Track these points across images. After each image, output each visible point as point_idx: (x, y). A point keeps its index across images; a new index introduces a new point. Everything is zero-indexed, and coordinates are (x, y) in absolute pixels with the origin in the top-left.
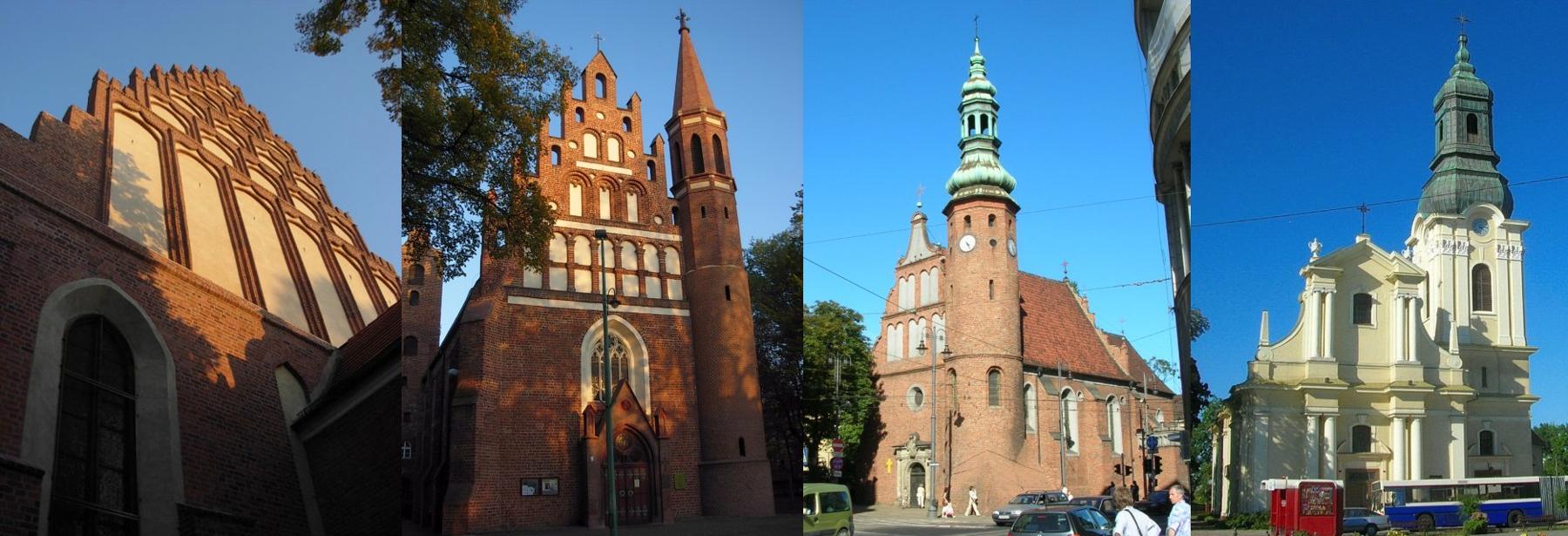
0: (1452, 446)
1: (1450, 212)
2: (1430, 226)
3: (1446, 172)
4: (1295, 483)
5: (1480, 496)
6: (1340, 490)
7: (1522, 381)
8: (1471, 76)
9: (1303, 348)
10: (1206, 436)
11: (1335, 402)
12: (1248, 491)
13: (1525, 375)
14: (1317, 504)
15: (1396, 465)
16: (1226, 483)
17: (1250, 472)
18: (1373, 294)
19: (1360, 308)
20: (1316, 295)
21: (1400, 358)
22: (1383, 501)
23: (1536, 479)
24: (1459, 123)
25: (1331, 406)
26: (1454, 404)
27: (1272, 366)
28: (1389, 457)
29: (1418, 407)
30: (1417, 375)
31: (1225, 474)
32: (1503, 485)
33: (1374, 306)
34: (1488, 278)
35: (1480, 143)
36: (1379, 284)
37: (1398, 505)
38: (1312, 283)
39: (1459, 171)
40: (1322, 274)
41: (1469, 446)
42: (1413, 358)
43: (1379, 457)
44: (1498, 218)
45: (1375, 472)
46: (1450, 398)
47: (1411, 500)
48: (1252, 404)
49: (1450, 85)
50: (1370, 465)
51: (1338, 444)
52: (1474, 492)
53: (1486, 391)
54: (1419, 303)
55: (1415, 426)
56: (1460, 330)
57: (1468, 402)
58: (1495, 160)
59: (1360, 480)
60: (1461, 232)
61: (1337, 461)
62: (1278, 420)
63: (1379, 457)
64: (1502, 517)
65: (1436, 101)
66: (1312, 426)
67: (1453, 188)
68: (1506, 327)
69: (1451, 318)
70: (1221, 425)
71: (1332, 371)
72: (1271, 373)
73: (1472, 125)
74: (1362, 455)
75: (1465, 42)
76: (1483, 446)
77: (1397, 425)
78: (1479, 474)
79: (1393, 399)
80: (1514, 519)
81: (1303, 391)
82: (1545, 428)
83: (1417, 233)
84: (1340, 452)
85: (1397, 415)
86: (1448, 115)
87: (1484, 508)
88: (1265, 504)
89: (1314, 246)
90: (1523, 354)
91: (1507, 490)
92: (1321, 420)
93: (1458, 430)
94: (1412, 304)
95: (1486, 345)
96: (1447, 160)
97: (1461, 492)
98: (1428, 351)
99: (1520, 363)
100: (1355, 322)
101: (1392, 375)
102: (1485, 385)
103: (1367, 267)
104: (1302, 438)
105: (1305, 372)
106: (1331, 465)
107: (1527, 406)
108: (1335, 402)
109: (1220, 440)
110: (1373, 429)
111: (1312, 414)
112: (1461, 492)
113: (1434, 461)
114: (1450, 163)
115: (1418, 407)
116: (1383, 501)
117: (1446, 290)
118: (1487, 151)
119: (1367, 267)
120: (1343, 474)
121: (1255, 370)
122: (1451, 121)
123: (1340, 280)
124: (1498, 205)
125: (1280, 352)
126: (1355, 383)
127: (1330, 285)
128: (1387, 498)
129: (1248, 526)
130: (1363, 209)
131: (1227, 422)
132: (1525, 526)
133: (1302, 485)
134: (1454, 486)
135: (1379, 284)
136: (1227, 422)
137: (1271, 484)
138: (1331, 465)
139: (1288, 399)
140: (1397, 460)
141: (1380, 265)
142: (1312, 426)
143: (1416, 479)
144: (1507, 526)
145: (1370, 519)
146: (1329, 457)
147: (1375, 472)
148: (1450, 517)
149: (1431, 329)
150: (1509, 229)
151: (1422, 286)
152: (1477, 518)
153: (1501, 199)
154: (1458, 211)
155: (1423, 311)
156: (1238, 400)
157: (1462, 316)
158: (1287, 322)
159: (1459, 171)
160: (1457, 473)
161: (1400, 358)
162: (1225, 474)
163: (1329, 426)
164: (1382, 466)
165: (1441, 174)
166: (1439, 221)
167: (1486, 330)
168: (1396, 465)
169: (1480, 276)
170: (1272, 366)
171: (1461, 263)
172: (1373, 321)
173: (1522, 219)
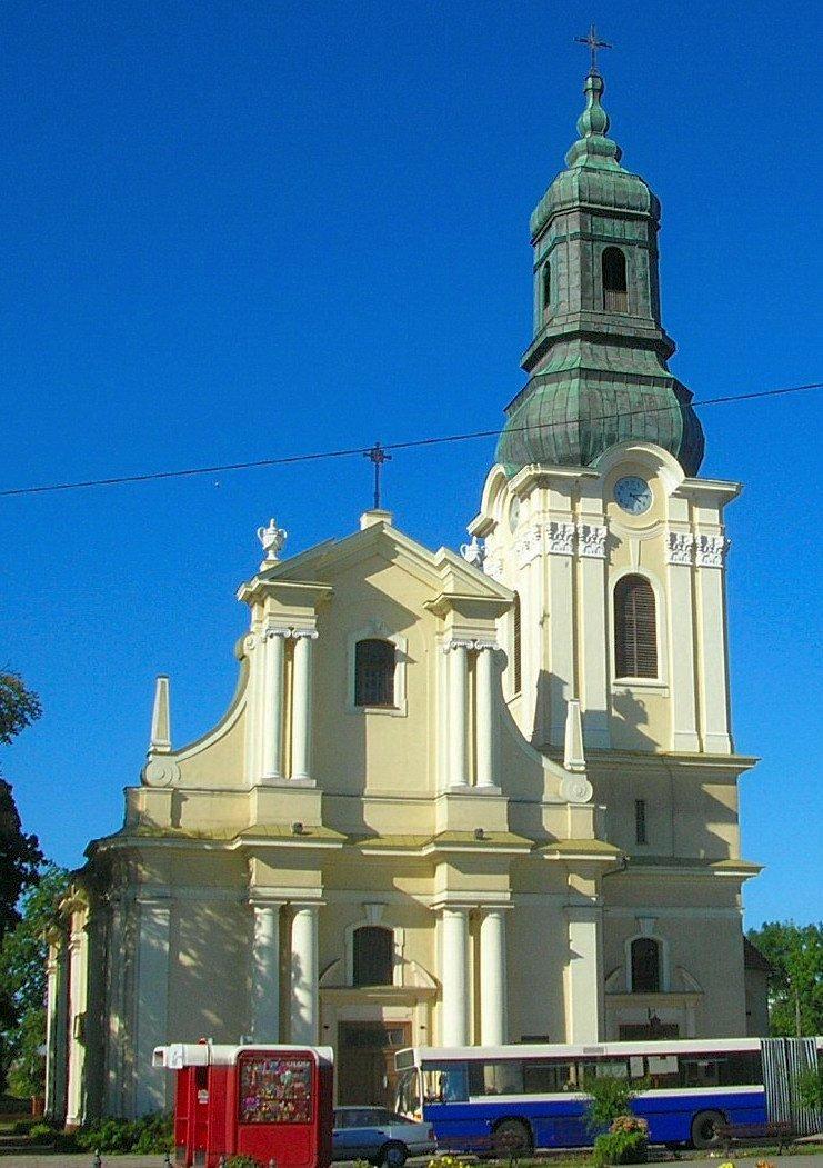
0: (569, 973)
1: (565, 462)
2: (523, 493)
3: (557, 376)
4: (228, 1053)
5: (631, 1082)
6: (324, 1069)
7: (723, 831)
8: (612, 165)
9: (246, 758)
10: (34, 951)
11: (315, 876)
12: (125, 1070)
13: (730, 817)
14: (275, 1100)
15: (448, 1014)
16: (77, 1053)
17: (130, 1028)
18: (399, 641)
19: (366, 672)
20: (274, 643)
21: (456, 779)
22: (421, 1091)
23: (753, 1044)
24: (584, 268)
25: (306, 884)
26: (575, 881)
27: (178, 797)
28: (433, 996)
29: (496, 887)
30: (494, 816)
31: (74, 1032)
32: (681, 1057)
33: (400, 667)
34: (648, 606)
35: (632, 312)
36: (413, 619)
37: (452, 1101)
38: (265, 618)
39: (586, 373)
40: (286, 598)
41: (606, 972)
42: (484, 780)
43: (412, 997)
44: (671, 475)
45: (402, 1030)
46: (567, 867)
47: (479, 1089)
48: (135, 881)
49: (567, 184)
50: (391, 1014)
51: (323, 966)
52: (619, 1071)
53: (643, 851)
54: (498, 660)
55: (490, 928)
56: (588, 719)
57: (605, 875)
58: (664, 349)
59: (370, 1045)
60: (590, 505)
61: (320, 1005)
62: (191, 917)
63: (412, 997)
64: (679, 1126)
65: (536, 220)
66: (264, 929)
67: (573, 409)
68: (687, 713)
69: (568, 693)
70: (65, 926)
71: (309, 810)
72: (176, 814)
73: (613, 273)
74: (373, 991)
75: (599, 92)
76: (637, 972)
77: (451, 925)
78: (628, 1033)
79: (443, 870)
80: (706, 1131)
81: (246, 853)
82: (773, 932)
83: (493, 507)
84: (325, 986)
85: (451, 905)
86: (560, 252)
87: (641, 1107)
88: (162, 1098)
89: (269, 537)
90: (725, 771)
91: (690, 1070)
92: (285, 914)
93: (583, 936)
94: (483, 662)
95: (644, 751)
96: (559, 349)
97: (590, 1073)
98: (518, 765)
99: (719, 792)
100: (360, 701)
101: (440, 818)
102: (641, 838)
103: (384, 581)
104: (242, 956)
105: (250, 811)
106: (305, 1013)
107: (735, 886)
108: (315, 876)
109: (65, 959)
110: (398, 934)
111: (264, 902)
112: (590, 1073)
113: (529, 1003)
114: (568, 356)
115: (496, 887)
116: (421, 1091)
117: (559, 636)
118: (647, 329)
119: (384, 581)
120: (333, 1031)
121: (142, 806)
122: (568, 265)
123: (326, 610)
124: (670, 447)
125: (194, 768)
126: (358, 834)
127: (303, 620)
128: (429, 1086)
129: (126, 1145)
130: (377, 455)
131: (80, 919)
132: (729, 1145)
133: (244, 1057)
134: (576, 1060)
135: (413, 619)
136: (80, 919)
137: (177, 1055)
138: (305, 1013)
139: (214, 871)
140: (452, 1001)
141: (413, 577)
142: (264, 929)
143: (492, 1043)
144: (691, 1146)
145: (391, 1131)
146: (301, 995)
147: (402, 1030)
148: (566, 1128)
149: (525, 717)
150: (694, 498)
151: (504, 623)
152: (625, 1130)
153: (678, 434)
154: (584, 461)
155: (507, 678)
156: (104, 872)
157: (592, 689)
158: (209, 702)
159: (586, 373)
160: (581, 1032)
161: (456, 779)
162: (74, 1032)
163: (301, 927)
164: (417, 1015)
165: (546, 379)
166: (543, 482)
167: (644, 719)
168: (448, 1014)
169: (632, 599)
170: (178, 797)
171: (591, 573)
172: (398, 699)
173: (723, 478)
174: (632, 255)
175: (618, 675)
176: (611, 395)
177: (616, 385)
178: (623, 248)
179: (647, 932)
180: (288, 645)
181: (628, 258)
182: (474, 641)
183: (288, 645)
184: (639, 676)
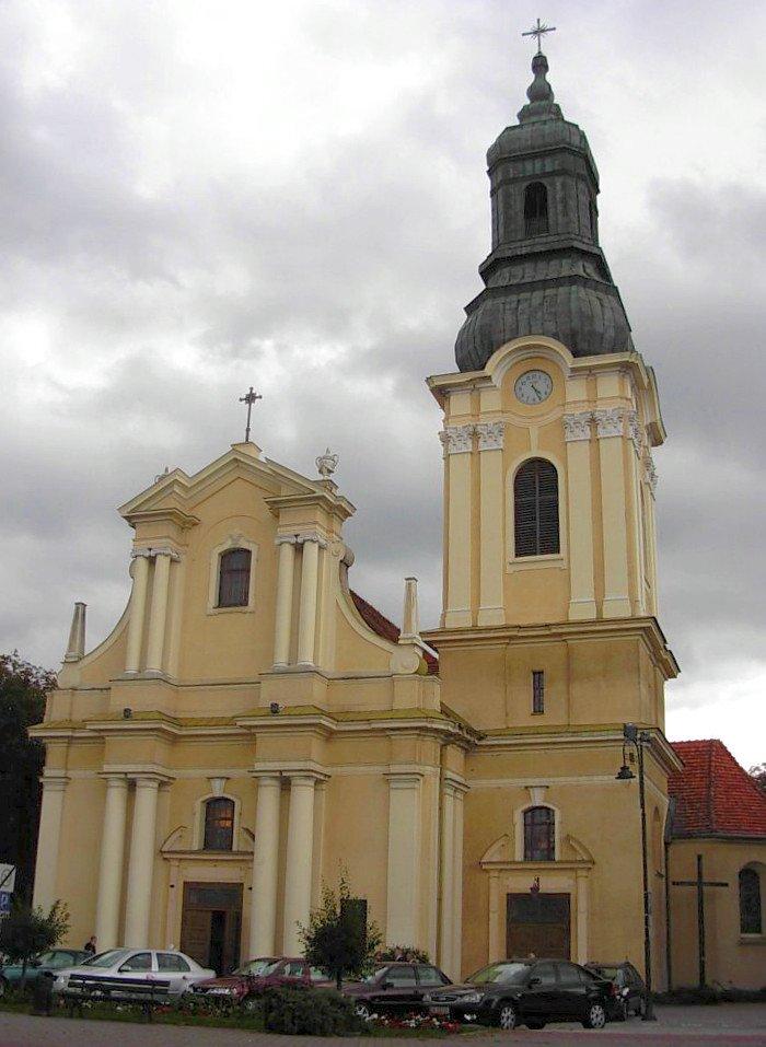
174: (553, 184)
175: (517, 556)
176: (514, 305)
177: (523, 296)
178: (544, 181)
179: (538, 799)
180: (152, 561)
181: (548, 188)
182: (296, 536)
183: (152, 561)
184: (542, 553)
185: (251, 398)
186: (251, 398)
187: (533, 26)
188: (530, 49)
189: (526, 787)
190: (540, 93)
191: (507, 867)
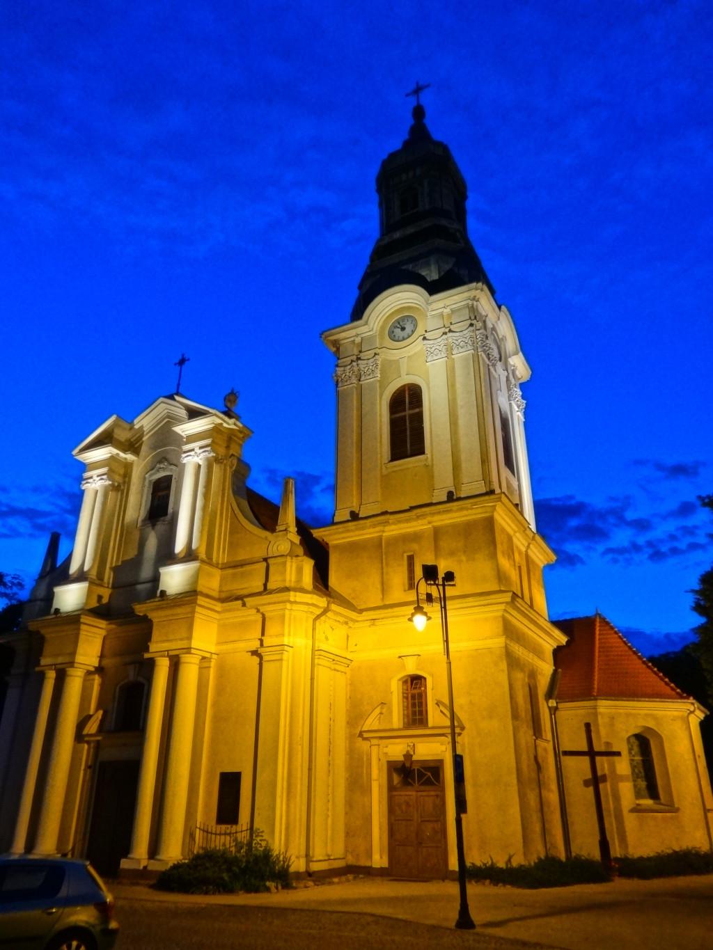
185: (182, 362)
186: (182, 362)
187: (412, 87)
188: (412, 101)
189: (400, 657)
190: (419, 132)
191: (388, 735)
